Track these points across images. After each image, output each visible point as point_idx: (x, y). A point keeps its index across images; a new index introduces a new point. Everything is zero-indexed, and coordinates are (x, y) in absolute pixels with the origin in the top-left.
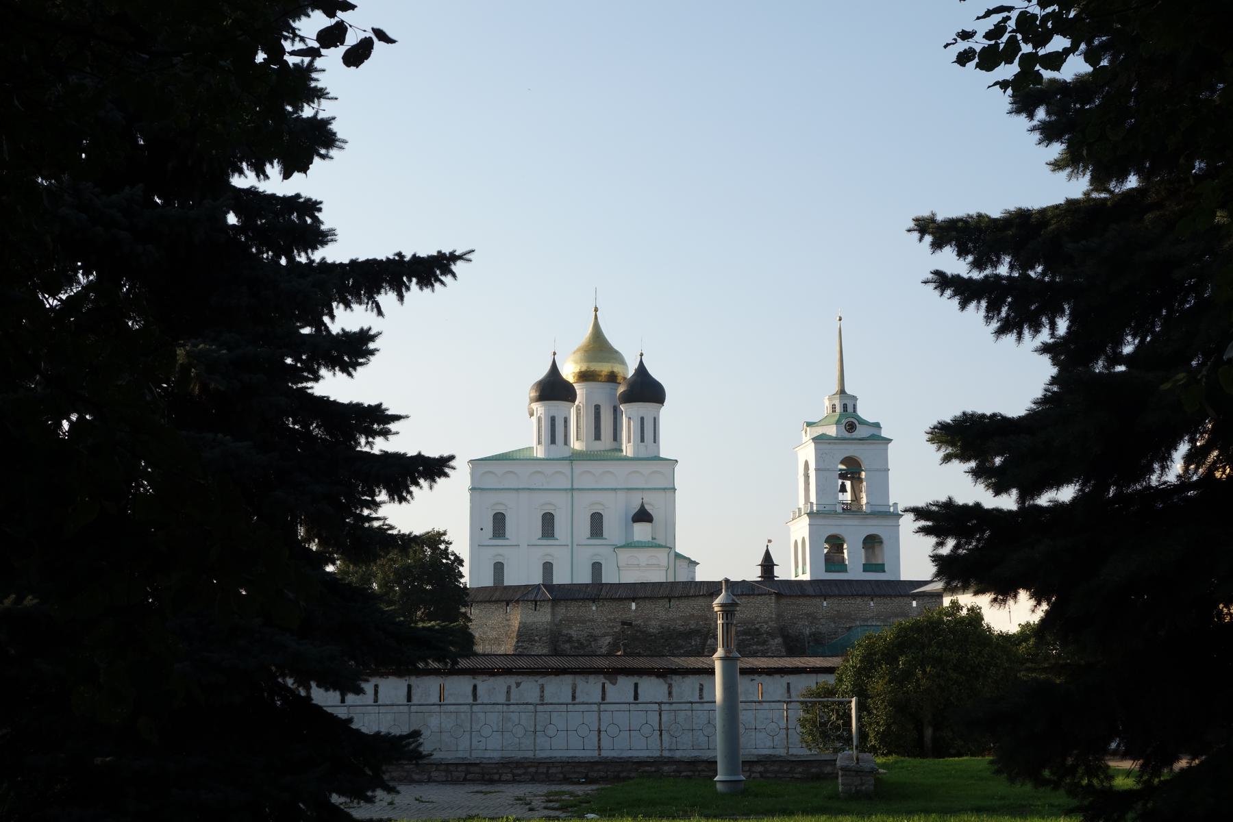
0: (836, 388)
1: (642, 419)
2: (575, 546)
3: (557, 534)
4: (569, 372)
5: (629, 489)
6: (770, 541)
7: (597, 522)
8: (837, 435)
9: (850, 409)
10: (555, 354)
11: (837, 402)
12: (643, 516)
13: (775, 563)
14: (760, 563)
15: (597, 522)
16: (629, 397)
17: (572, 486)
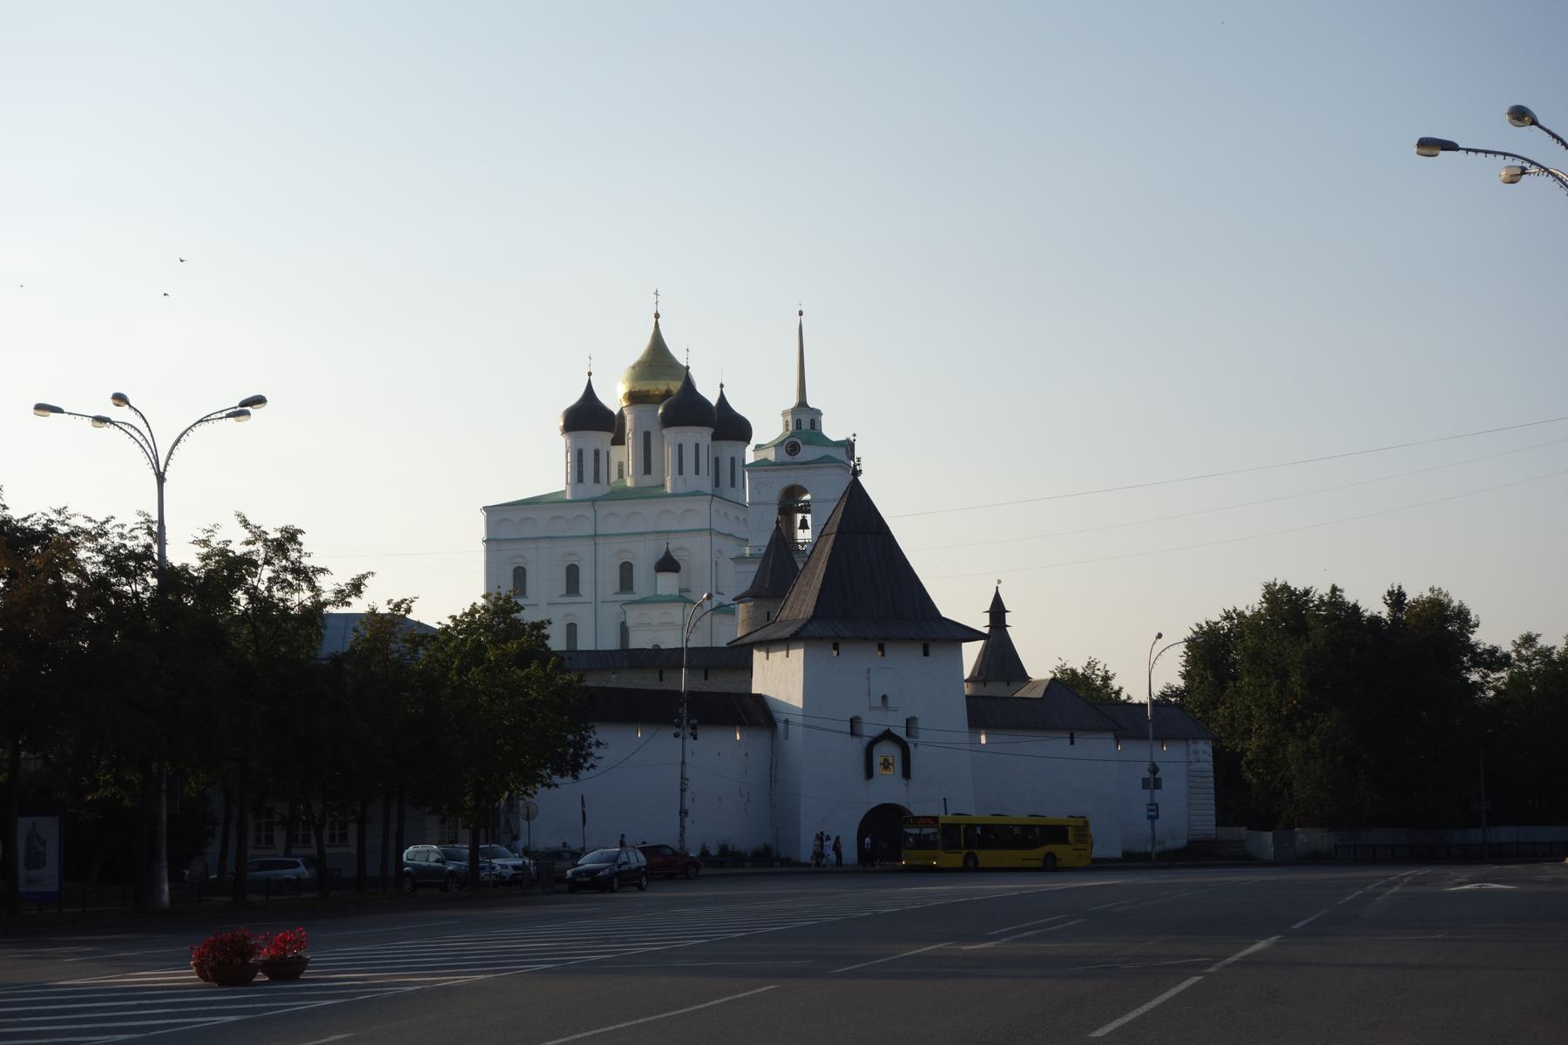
0: (793, 401)
1: (680, 446)
2: (599, 604)
3: (581, 591)
4: (613, 397)
5: (658, 532)
6: (999, 582)
7: (626, 570)
8: (776, 459)
9: (806, 425)
10: (590, 374)
11: (789, 418)
12: (668, 564)
13: (1007, 609)
14: (988, 609)
15: (626, 570)
16: (669, 421)
17: (595, 531)
